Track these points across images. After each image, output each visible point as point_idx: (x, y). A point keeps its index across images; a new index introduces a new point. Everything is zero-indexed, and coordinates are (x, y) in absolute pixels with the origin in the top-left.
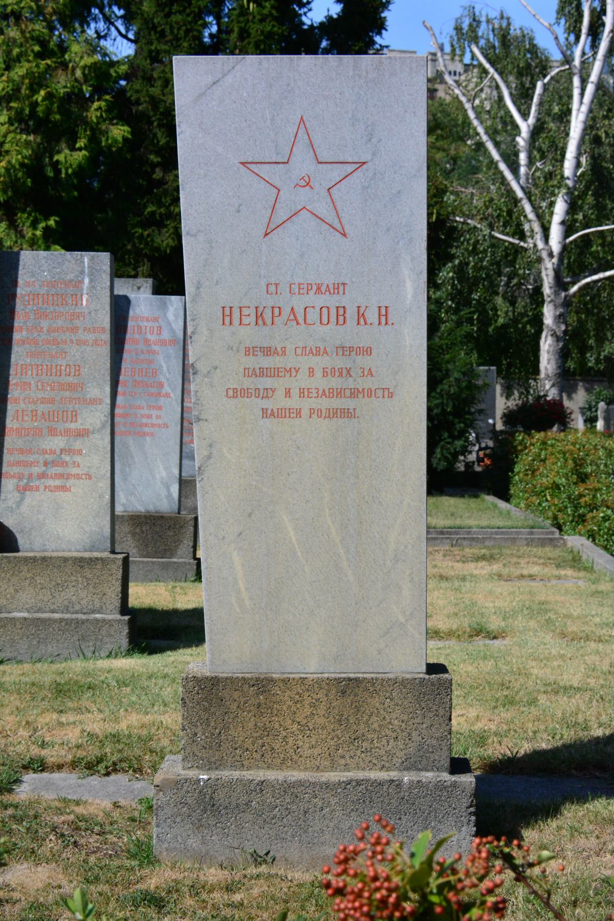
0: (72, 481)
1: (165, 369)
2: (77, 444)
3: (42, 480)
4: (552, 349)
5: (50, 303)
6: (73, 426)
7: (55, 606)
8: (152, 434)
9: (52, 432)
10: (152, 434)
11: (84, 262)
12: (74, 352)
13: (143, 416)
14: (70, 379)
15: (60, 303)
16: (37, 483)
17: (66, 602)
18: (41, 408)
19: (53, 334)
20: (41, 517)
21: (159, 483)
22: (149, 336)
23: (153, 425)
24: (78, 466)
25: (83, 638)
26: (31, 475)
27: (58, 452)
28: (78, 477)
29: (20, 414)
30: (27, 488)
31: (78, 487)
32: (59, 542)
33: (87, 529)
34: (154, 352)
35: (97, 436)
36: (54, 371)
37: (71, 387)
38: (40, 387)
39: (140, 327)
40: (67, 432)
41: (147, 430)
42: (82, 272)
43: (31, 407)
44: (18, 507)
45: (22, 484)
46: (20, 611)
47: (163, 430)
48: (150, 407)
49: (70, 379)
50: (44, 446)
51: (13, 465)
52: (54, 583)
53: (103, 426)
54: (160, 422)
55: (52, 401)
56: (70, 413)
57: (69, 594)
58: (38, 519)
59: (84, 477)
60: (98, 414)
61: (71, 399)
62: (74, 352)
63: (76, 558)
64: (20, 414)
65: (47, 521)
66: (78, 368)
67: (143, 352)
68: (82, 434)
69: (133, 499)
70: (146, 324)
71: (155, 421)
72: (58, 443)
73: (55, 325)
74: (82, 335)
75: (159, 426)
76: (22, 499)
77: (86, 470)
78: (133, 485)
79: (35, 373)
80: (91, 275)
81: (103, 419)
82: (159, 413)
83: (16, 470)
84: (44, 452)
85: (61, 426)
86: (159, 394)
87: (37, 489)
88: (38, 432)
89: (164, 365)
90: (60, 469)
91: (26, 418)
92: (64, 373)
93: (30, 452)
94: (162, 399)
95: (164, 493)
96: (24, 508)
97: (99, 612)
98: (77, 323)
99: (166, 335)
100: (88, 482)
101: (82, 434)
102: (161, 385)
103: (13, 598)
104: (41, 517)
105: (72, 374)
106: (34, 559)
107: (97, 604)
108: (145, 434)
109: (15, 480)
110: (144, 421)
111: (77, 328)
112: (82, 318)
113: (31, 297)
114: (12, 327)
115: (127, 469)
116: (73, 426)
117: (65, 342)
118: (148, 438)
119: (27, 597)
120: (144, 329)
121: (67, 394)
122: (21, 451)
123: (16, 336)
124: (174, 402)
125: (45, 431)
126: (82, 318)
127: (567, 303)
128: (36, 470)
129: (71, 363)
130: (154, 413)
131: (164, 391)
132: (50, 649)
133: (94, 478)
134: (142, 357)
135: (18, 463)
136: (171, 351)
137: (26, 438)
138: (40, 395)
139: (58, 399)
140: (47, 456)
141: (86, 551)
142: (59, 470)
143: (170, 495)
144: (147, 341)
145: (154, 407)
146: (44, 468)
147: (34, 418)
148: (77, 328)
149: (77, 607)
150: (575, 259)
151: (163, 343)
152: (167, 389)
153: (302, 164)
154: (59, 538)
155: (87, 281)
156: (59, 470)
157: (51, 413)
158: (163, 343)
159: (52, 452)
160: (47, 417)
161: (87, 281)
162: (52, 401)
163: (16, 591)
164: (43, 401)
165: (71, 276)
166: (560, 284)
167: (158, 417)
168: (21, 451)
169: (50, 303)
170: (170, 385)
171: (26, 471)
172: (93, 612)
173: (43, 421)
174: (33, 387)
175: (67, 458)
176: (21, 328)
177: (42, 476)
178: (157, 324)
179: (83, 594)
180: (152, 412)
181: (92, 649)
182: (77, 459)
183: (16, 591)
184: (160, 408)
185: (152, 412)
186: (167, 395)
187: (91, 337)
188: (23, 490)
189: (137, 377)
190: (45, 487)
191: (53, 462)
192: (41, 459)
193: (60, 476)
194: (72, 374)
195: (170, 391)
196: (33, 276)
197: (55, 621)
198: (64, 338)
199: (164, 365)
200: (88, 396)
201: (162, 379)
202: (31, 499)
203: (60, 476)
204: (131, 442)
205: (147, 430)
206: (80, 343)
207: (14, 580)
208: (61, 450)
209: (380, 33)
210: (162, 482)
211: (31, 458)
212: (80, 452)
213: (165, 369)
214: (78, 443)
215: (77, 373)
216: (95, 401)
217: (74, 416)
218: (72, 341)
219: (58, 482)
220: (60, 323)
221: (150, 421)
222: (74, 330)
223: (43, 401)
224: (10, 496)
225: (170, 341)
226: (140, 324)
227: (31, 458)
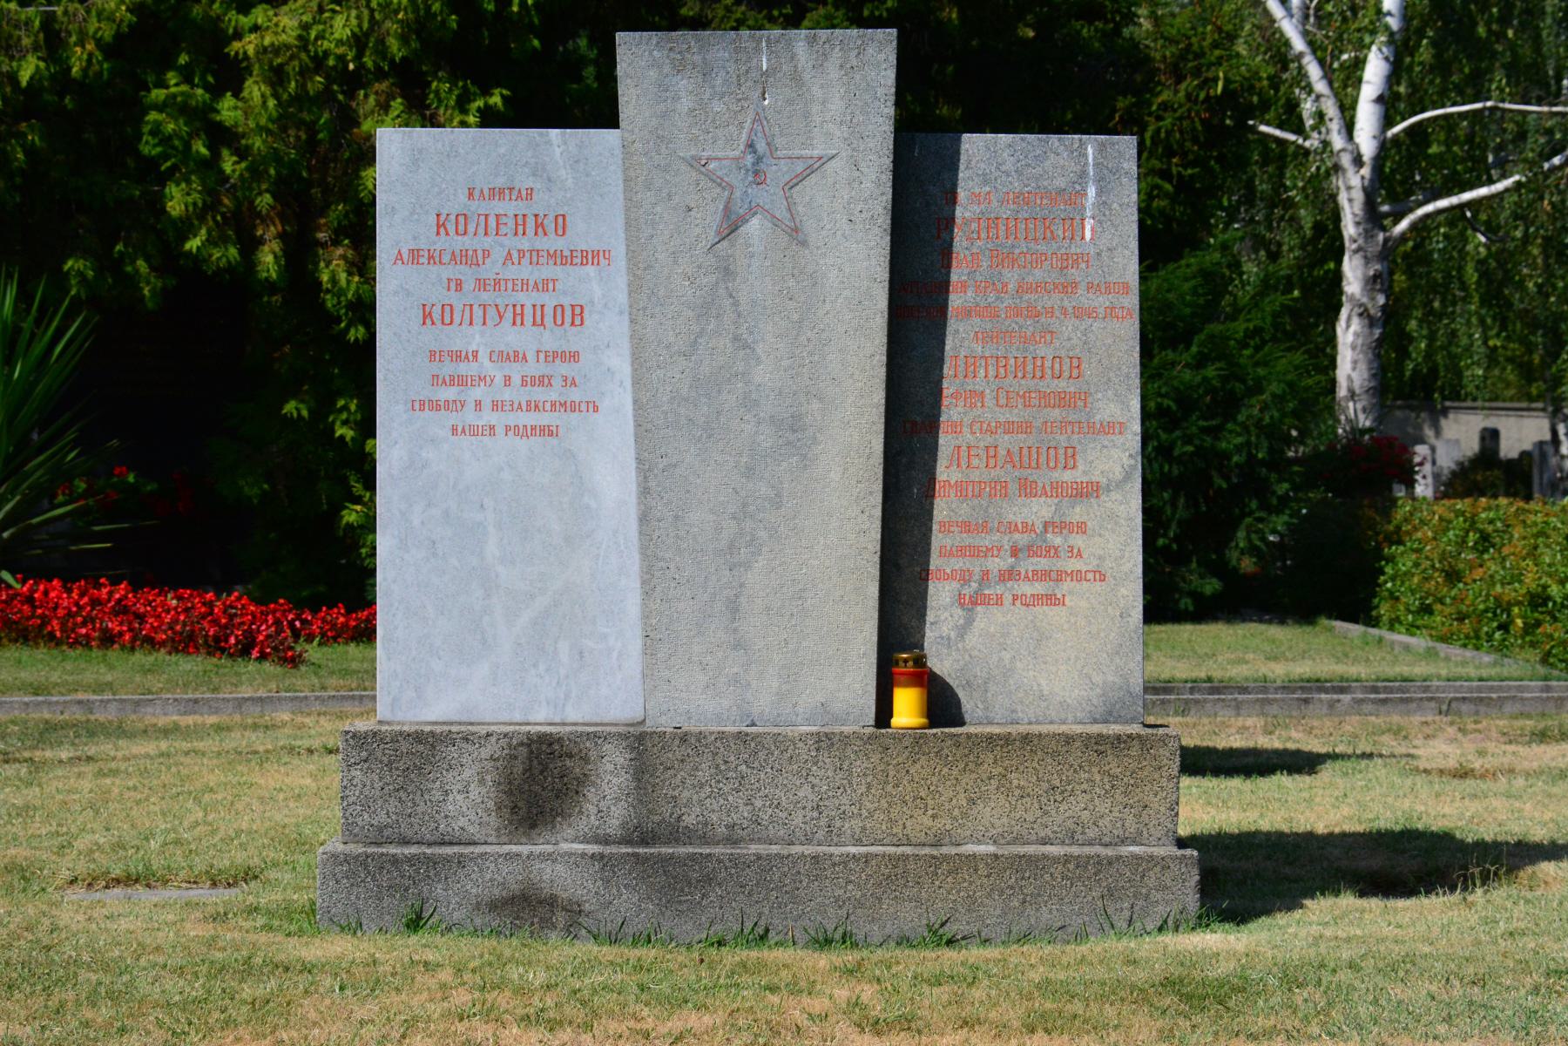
0: (1067, 585)
2: (1077, 513)
3: (1009, 584)
4: (1360, 341)
5: (1022, 236)
6: (1067, 476)
9: (1028, 489)
11: (1085, 155)
12: (1069, 329)
14: (1062, 384)
15: (1040, 234)
16: (999, 589)
17: (1070, 823)
18: (1005, 441)
19: (1026, 297)
20: (1007, 656)
24: (1080, 554)
25: (1111, 893)
26: (986, 574)
27: (1039, 528)
28: (1078, 576)
29: (964, 454)
30: (977, 600)
31: (1079, 596)
32: (1044, 704)
33: (1098, 679)
35: (1115, 495)
36: (1030, 368)
37: (1063, 401)
38: (1003, 401)
40: (1057, 489)
42: (1083, 174)
43: (989, 440)
44: (961, 636)
45: (967, 591)
46: (979, 842)
49: (1062, 384)
50: (1012, 517)
51: (951, 554)
52: (1045, 786)
53: (1127, 477)
55: (1025, 427)
56: (1061, 451)
57: (1075, 808)
58: (1001, 659)
59: (1090, 576)
60: (1116, 453)
61: (1064, 424)
62: (1069, 329)
63: (1089, 736)
64: (964, 454)
65: (1018, 664)
66: (1077, 364)
68: (1087, 491)
72: (1039, 510)
73: (1030, 279)
74: (1084, 298)
76: (969, 622)
79: (992, 373)
80: (1099, 180)
81: (1127, 462)
83: (958, 564)
84: (1012, 528)
85: (1043, 477)
87: (999, 601)
88: (999, 489)
90: (1043, 561)
91: (975, 462)
93: (984, 528)
96: (972, 639)
97: (1134, 843)
101: (1087, 491)
103: (965, 815)
105: (1066, 374)
106: (1007, 739)
107: (1131, 826)
109: (955, 585)
111: (1075, 285)
113: (983, 224)
114: (947, 282)
116: (1067, 476)
117: (1050, 312)
119: (994, 813)
121: (1056, 414)
122: (966, 527)
123: (955, 301)
125: (1013, 488)
126: (1083, 266)
127: (1388, 252)
128: (995, 564)
129: (1063, 353)
132: (1046, 916)
133: (1109, 579)
135: (962, 551)
137: (976, 501)
138: (1004, 416)
139: (1038, 423)
140: (1017, 536)
141: (1095, 721)
142: (1042, 563)
147: (992, 462)
148: (1075, 285)
150: (1397, 175)
154: (1041, 697)
155: (1092, 191)
156: (1042, 563)
157: (1025, 451)
159: (1027, 528)
161: (1092, 191)
162: (1025, 427)
163: (972, 802)
164: (1009, 428)
165: (1060, 183)
166: (1373, 218)
168: (966, 527)
169: (1022, 236)
171: (976, 566)
172: (1124, 841)
174: (989, 402)
175: (1058, 541)
176: (964, 286)
177: (1009, 575)
179: (1102, 807)
181: (1127, 914)
182: (1078, 541)
183: (972, 802)
187: (1101, 302)
188: (970, 603)
190: (1015, 598)
191: (1029, 548)
193: (1044, 575)
194: (1066, 374)
196: (985, 182)
197: (1055, 860)
198: (1049, 304)
200: (1098, 417)
202: (987, 620)
203: (1044, 575)
206: (1080, 313)
207: (966, 779)
208: (1046, 524)
211: (986, 541)
212: (1082, 528)
214: (1078, 510)
216: (1110, 428)
217: (1070, 458)
218: (1064, 312)
219: (1039, 588)
220: (1038, 274)
222: (1068, 288)
223: (1009, 428)
224: (947, 614)
227: (986, 541)
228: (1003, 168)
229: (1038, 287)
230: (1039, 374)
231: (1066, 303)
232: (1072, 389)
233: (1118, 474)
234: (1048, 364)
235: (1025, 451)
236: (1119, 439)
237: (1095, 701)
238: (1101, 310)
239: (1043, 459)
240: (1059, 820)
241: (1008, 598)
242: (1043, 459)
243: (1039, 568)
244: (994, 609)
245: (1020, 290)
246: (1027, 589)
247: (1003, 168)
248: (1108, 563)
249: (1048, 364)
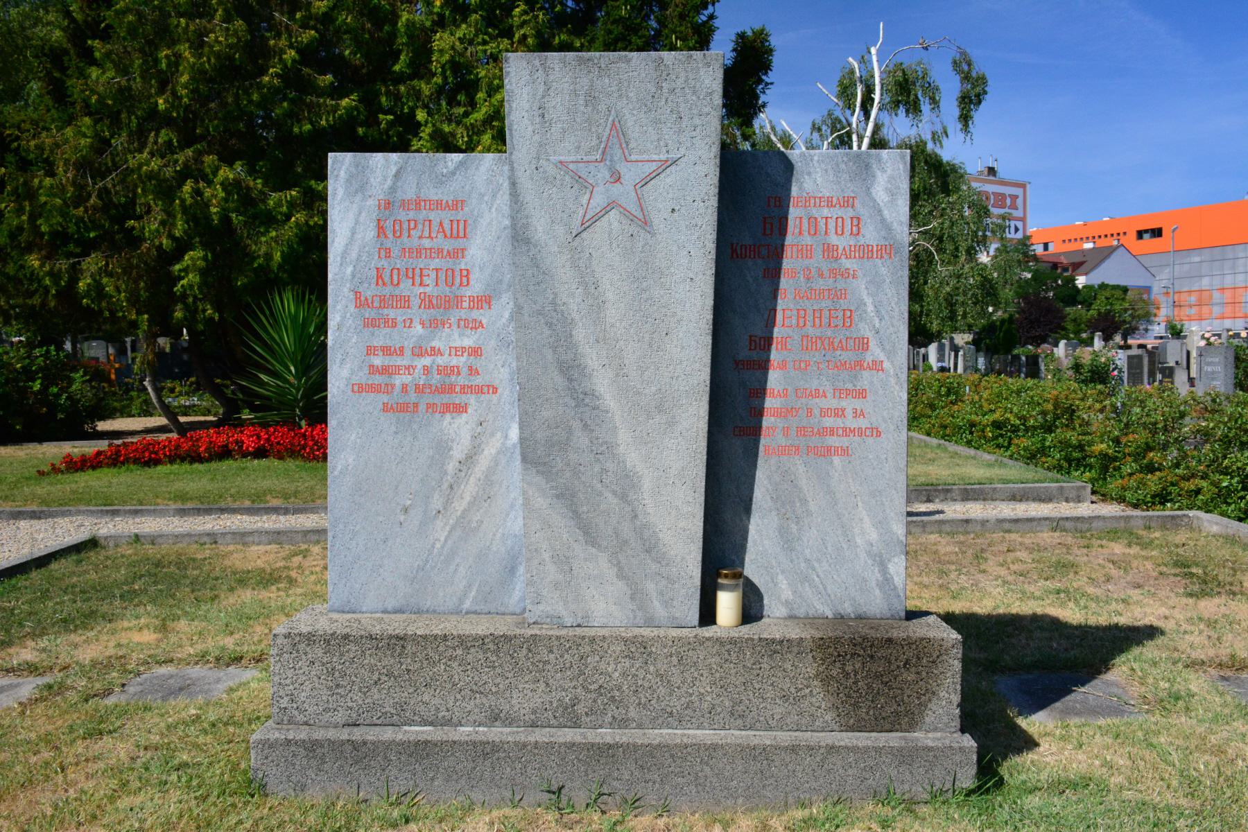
1: (870, 308)
8: (845, 452)
10: (845, 452)
13: (824, 413)
21: (863, 555)
22: (833, 239)
23: (847, 432)
34: (845, 274)
39: (813, 220)
41: (833, 441)
47: (870, 440)
48: (840, 393)
54: (863, 423)
67: (821, 275)
69: (808, 591)
70: (826, 212)
71: (851, 423)
75: (860, 432)
78: (807, 561)
82: (858, 404)
86: (860, 364)
89: (868, 301)
94: (866, 374)
95: (874, 575)
99: (870, 235)
102: (863, 345)
108: (829, 451)
110: (829, 422)
115: (794, 528)
118: (836, 460)
120: (822, 223)
124: (893, 381)
130: (849, 404)
131: (869, 358)
134: (820, 284)
136: (883, 271)
143: (887, 580)
144: (829, 250)
145: (848, 393)
151: (866, 253)
152: (875, 352)
158: (866, 253)
167: (858, 414)
170: (881, 344)
178: (850, 213)
180: (844, 404)
184: (862, 394)
185: (844, 404)
186: (877, 366)
189: (810, 330)
195: (882, 357)
199: (868, 301)
201: (865, 330)
204: (801, 469)
205: (833, 441)
209: (766, 74)
210: (869, 553)
213: (870, 308)
221: (839, 422)
225: (881, 249)
226: (815, 212)
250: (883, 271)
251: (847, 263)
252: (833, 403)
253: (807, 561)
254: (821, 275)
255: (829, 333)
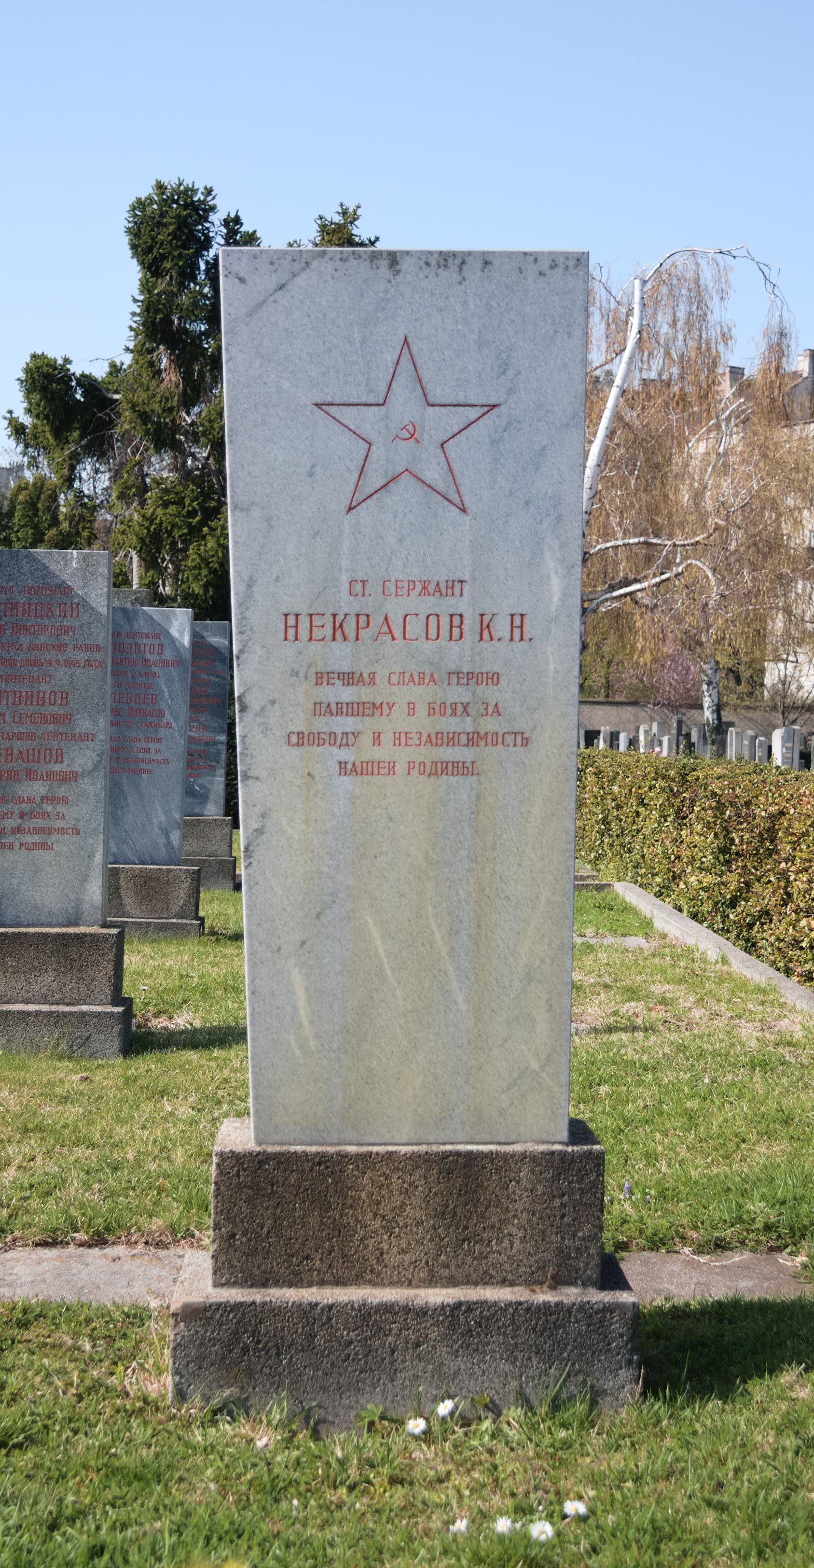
0: (54, 837)
1: (166, 694)
2: (62, 791)
3: (18, 836)
5: (33, 615)
6: (57, 768)
7: (30, 995)
8: (150, 772)
9: (31, 775)
10: (150, 772)
12: (61, 674)
13: (139, 750)
15: (44, 613)
16: (11, 839)
17: (44, 990)
18: (18, 745)
19: (34, 653)
20: (15, 882)
21: (157, 829)
22: (148, 656)
23: (151, 761)
27: (38, 800)
28: (62, 831)
32: (37, 913)
34: (154, 675)
35: (87, 780)
36: (35, 698)
37: (56, 719)
38: (17, 719)
39: (137, 645)
40: (50, 775)
41: (143, 766)
48: (147, 739)
49: (55, 709)
53: (96, 767)
54: (159, 756)
55: (30, 736)
56: (54, 752)
59: (70, 831)
60: (89, 753)
61: (56, 734)
62: (61, 674)
66: (65, 696)
67: (140, 675)
68: (68, 778)
69: (125, 847)
70: (144, 641)
71: (153, 756)
72: (38, 789)
73: (37, 642)
77: (73, 822)
78: (126, 831)
79: (11, 701)
82: (158, 746)
84: (21, 800)
85: (44, 768)
86: (159, 724)
87: (11, 847)
89: (166, 690)
90: (40, 821)
92: (47, 701)
95: (162, 840)
98: (66, 639)
99: (168, 655)
100: (75, 838)
101: (68, 778)
102: (162, 714)
104: (15, 882)
105: (58, 702)
110: (141, 755)
111: (66, 645)
112: (71, 633)
116: (57, 768)
117: (49, 663)
118: (144, 776)
120: (142, 647)
121: (51, 727)
124: (177, 734)
125: (22, 775)
126: (71, 633)
128: (11, 823)
129: (57, 689)
130: (153, 746)
131: (165, 721)
133: (82, 833)
134: (140, 680)
136: (174, 674)
139: (39, 734)
140: (24, 805)
143: (169, 843)
144: (145, 661)
145: (153, 740)
146: (19, 821)
148: (66, 645)
149: (57, 997)
151: (165, 664)
152: (168, 718)
153: (405, 406)
154: (36, 907)
157: (31, 752)
159: (30, 800)
160: (25, 756)
162: (30, 736)
164: (21, 736)
167: (157, 751)
169: (33, 615)
170: (171, 713)
173: (20, 761)
175: (50, 809)
177: (18, 830)
178: (157, 642)
180: (150, 746)
182: (62, 809)
184: (159, 740)
185: (150, 746)
186: (169, 726)
187: (82, 656)
189: (133, 704)
190: (21, 845)
191: (31, 813)
192: (16, 809)
193: (40, 831)
194: (58, 702)
198: (48, 658)
199: (166, 690)
201: (164, 707)
203: (40, 831)
205: (143, 766)
206: (69, 663)
208: (42, 798)
210: (160, 828)
212: (65, 801)
213: (166, 694)
214: (63, 789)
215: (64, 702)
217: (59, 756)
218: (58, 662)
219: (36, 838)
220: (43, 639)
221: (147, 756)
223: (21, 736)
225: (173, 662)
226: (139, 641)
228: (22, 571)
229: (43, 647)
230: (41, 702)
231: (60, 657)
232: (62, 712)
233: (89, 765)
234: (47, 696)
235: (31, 752)
236: (91, 745)
237: (70, 911)
238: (82, 662)
239: (42, 756)
240: (37, 988)
241: (17, 844)
242: (42, 756)
243: (37, 826)
244: (8, 852)
245: (31, 648)
246: (29, 839)
247: (22, 571)
248: (82, 823)
249: (47, 696)
250: (174, 674)
251: (154, 669)
252: (144, 745)
253: (126, 831)
254: (140, 675)
255: (144, 707)
